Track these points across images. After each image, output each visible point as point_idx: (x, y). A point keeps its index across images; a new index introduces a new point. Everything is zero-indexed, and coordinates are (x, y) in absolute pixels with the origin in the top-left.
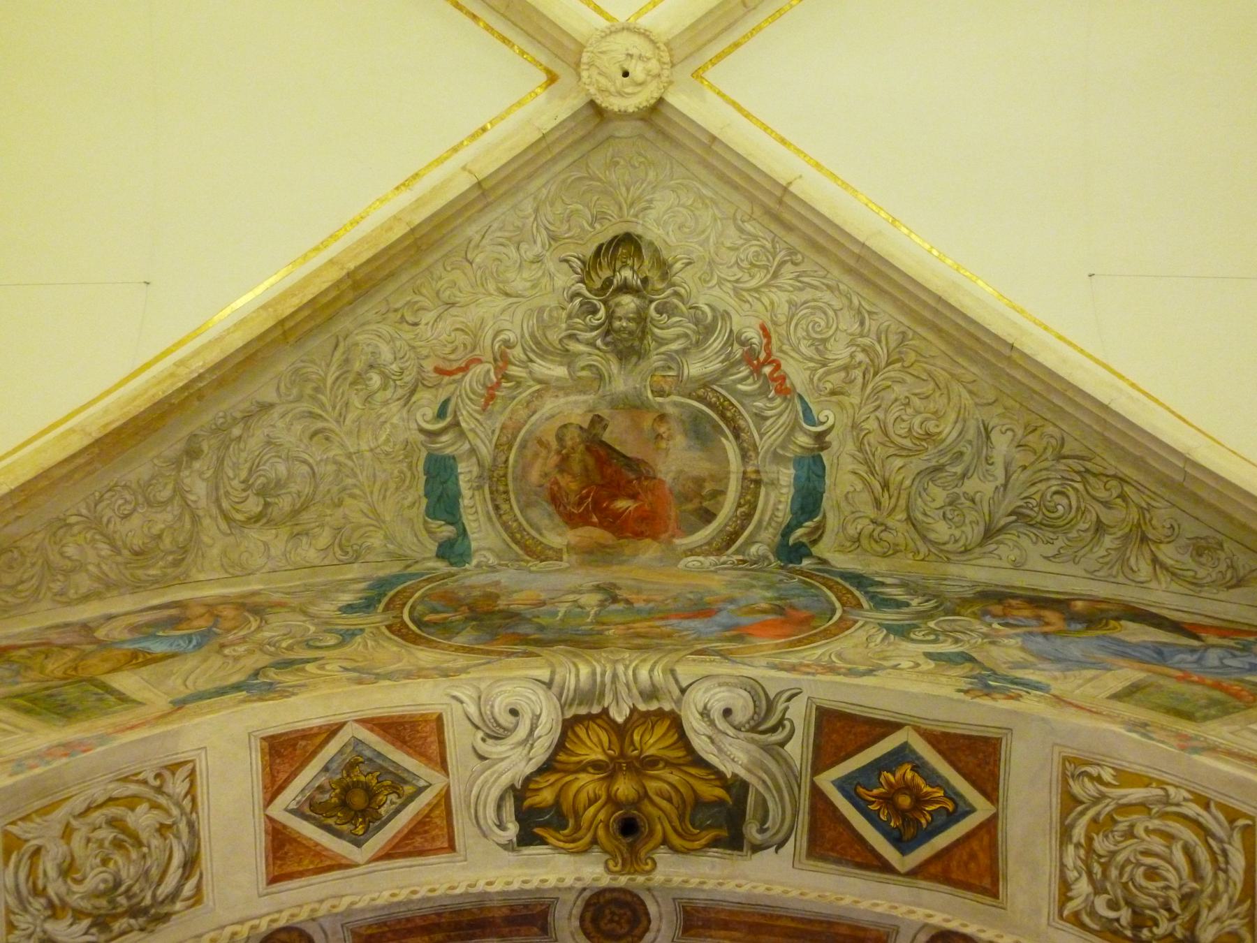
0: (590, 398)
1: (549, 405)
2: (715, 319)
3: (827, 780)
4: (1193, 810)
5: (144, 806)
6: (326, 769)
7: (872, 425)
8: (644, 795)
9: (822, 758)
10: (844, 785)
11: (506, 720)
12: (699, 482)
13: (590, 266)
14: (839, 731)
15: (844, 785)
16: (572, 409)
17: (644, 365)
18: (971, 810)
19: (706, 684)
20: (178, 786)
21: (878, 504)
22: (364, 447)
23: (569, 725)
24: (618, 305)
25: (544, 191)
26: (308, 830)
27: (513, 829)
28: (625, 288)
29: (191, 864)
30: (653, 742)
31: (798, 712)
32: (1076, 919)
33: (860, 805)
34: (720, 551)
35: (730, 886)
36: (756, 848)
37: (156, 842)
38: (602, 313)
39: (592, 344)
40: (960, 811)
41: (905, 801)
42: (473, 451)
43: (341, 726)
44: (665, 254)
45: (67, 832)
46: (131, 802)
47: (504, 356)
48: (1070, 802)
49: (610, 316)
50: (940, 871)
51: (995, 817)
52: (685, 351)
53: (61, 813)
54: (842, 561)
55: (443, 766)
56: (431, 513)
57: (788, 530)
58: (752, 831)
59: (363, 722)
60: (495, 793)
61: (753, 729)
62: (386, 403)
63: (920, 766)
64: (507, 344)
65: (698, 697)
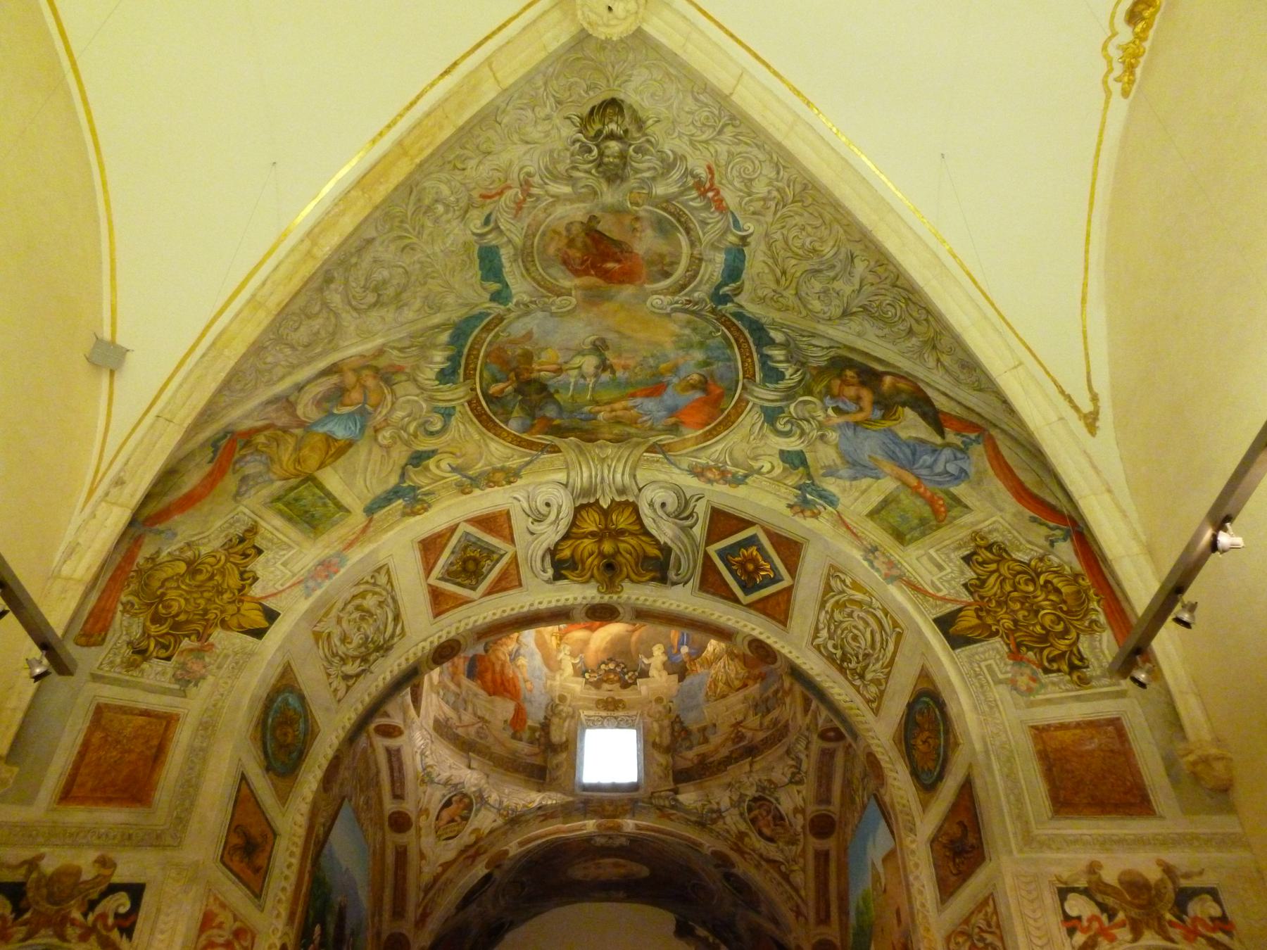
0: (588, 205)
1: (560, 210)
2: (675, 159)
3: (713, 550)
4: (880, 614)
5: (369, 596)
6: (453, 552)
7: (778, 236)
8: (618, 552)
9: (712, 537)
10: (723, 554)
11: (544, 510)
12: (662, 256)
14: (723, 522)
15: (723, 554)
16: (577, 212)
17: (625, 186)
18: (782, 580)
19: (653, 487)
20: (382, 579)
21: (778, 282)
22: (437, 249)
23: (578, 510)
24: (607, 147)
25: (551, 69)
26: (449, 587)
27: (550, 572)
28: (612, 136)
29: (397, 618)
30: (622, 521)
31: (701, 509)
32: (818, 648)
33: (728, 565)
34: (674, 294)
35: (658, 604)
36: (674, 584)
38: (595, 152)
39: (588, 172)
40: (776, 579)
41: (751, 567)
42: (510, 241)
43: (457, 525)
44: (640, 114)
45: (339, 621)
46: (363, 595)
47: (527, 182)
48: (828, 588)
49: (601, 154)
52: (654, 179)
53: (334, 612)
54: (753, 309)
55: (512, 541)
56: (485, 278)
57: (719, 287)
58: (672, 574)
59: (468, 521)
60: (540, 553)
61: (676, 517)
62: (449, 221)
63: (761, 549)
64: (529, 175)
65: (648, 494)
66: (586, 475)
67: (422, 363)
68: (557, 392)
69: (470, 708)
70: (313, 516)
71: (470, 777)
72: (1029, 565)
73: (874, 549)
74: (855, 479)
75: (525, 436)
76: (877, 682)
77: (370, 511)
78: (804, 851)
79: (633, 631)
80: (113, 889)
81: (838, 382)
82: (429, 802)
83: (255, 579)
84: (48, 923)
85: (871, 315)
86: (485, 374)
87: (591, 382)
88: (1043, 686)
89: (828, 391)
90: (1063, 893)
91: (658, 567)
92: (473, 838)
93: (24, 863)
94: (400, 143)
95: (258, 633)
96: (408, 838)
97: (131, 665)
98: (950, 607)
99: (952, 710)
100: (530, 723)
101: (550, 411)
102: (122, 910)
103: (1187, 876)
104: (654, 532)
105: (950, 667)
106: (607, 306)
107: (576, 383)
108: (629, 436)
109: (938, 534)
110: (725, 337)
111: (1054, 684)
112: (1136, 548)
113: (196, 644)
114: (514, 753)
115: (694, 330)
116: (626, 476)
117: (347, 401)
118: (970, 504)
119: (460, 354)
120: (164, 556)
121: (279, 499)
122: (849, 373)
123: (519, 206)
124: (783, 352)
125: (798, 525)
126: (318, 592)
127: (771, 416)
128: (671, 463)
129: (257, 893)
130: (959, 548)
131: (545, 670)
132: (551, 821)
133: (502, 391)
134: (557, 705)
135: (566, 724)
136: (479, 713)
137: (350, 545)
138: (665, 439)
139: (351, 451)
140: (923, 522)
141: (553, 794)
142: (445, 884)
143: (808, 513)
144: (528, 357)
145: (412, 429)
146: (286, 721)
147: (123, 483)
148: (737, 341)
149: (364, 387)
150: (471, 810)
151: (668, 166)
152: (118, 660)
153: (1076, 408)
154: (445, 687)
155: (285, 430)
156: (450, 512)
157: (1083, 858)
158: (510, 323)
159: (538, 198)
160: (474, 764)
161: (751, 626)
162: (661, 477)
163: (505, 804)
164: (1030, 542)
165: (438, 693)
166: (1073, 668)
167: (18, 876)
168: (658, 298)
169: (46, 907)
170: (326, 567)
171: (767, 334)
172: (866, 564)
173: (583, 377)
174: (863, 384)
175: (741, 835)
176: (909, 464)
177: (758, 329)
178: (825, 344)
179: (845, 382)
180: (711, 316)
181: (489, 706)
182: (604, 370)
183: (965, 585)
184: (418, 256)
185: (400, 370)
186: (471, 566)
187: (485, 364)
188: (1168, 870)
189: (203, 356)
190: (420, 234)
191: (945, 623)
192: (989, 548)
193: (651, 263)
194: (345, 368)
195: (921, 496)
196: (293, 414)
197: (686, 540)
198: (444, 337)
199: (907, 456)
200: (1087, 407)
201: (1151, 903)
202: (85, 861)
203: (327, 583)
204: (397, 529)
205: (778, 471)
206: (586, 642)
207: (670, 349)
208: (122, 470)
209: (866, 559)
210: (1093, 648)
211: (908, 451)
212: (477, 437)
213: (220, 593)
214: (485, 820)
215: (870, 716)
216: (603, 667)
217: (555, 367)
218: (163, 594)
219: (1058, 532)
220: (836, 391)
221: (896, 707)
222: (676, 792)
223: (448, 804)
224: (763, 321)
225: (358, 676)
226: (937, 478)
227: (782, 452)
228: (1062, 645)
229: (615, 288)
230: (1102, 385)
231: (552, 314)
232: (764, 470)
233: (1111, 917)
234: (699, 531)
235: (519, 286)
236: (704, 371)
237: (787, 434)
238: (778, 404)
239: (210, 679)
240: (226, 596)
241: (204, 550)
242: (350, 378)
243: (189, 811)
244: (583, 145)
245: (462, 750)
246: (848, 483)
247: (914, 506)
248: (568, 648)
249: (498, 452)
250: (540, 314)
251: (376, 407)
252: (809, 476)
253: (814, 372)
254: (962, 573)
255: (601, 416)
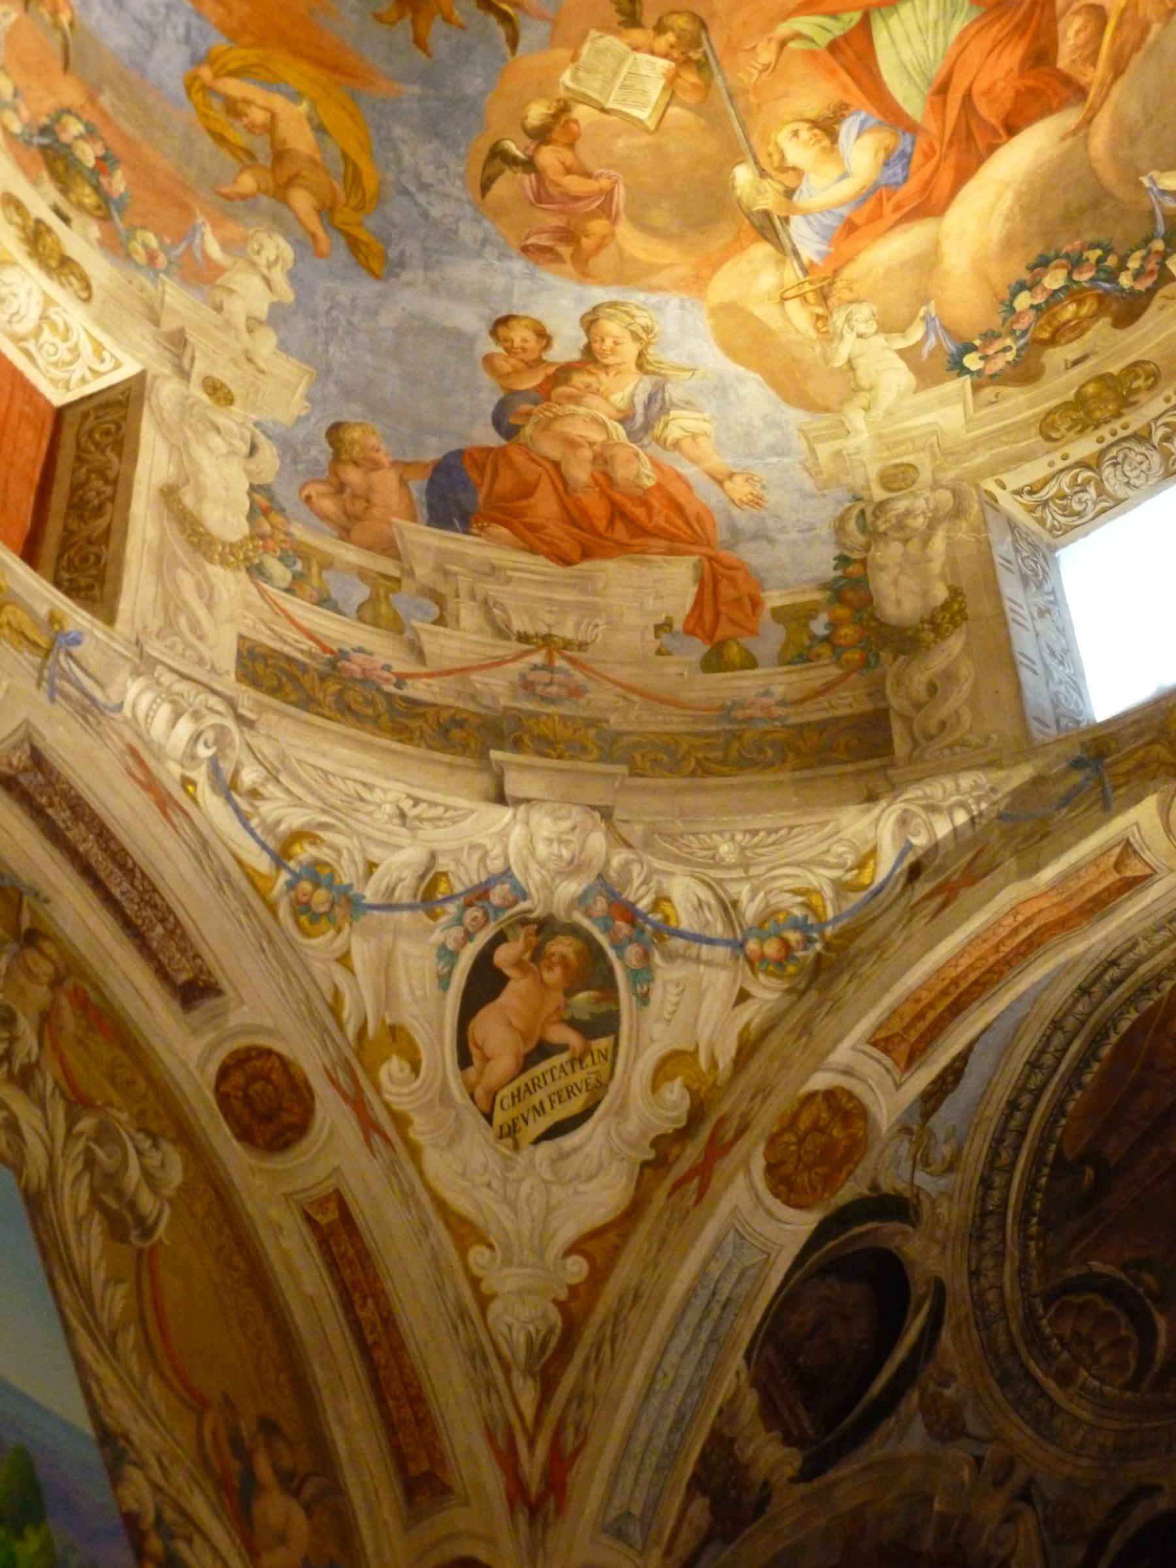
69: (469, 616)
71: (531, 839)
79: (1088, 121)
82: (387, 994)
92: (675, 1094)
96: (333, 1146)
100: (774, 599)
114: (725, 712)
131: (795, 416)
132: (967, 896)
134: (881, 506)
135: (938, 544)
136: (520, 624)
141: (937, 789)
142: (617, 1317)
150: (609, 987)
154: (294, 553)
160: (515, 784)
163: (751, 910)
165: (257, 571)
181: (569, 596)
206: (928, 262)
214: (692, 1009)
216: (1023, 301)
223: (484, 983)
245: (463, 749)
248: (863, 312)
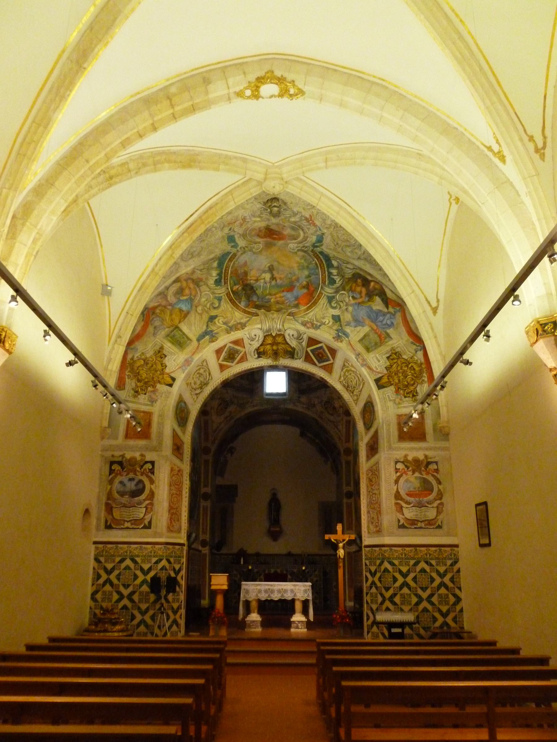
1: (256, 224)
3: (309, 349)
4: (359, 376)
8: (278, 349)
9: (309, 345)
10: (312, 351)
11: (254, 337)
12: (293, 236)
13: (265, 204)
14: (312, 341)
16: (263, 224)
17: (280, 218)
18: (330, 360)
20: (205, 364)
21: (335, 245)
23: (265, 337)
26: (225, 363)
27: (257, 356)
28: (275, 206)
29: (210, 374)
30: (279, 340)
31: (305, 337)
33: (314, 355)
37: (204, 373)
40: (328, 360)
41: (321, 356)
42: (238, 233)
43: (226, 345)
46: (199, 369)
48: (344, 365)
50: (324, 368)
51: (333, 363)
53: (192, 376)
55: (244, 347)
57: (314, 244)
58: (296, 356)
59: (231, 342)
63: (324, 350)
64: (245, 217)
65: (288, 332)
66: (267, 325)
67: (209, 277)
68: (257, 289)
70: (180, 342)
72: (407, 360)
73: (359, 354)
74: (356, 327)
75: (247, 309)
76: (357, 396)
77: (198, 340)
78: (342, 419)
80: (147, 462)
81: (354, 285)
83: (166, 366)
84: (131, 471)
85: (367, 261)
86: (231, 282)
87: (268, 285)
88: (404, 402)
89: (351, 290)
90: (396, 463)
91: (291, 354)
93: (120, 456)
94: (200, 217)
95: (171, 385)
97: (135, 397)
98: (380, 375)
99: (376, 408)
101: (255, 299)
102: (151, 467)
103: (431, 458)
104: (290, 343)
105: (377, 395)
106: (274, 249)
107: (263, 286)
108: (282, 309)
109: (380, 348)
110: (316, 264)
111: (407, 401)
112: (439, 357)
113: (153, 389)
115: (305, 260)
116: (281, 326)
117: (184, 294)
118: (392, 337)
119: (222, 272)
120: (135, 358)
121: (168, 336)
122: (359, 281)
123: (241, 225)
124: (336, 271)
125: (336, 345)
126: (186, 371)
127: (330, 299)
128: (295, 320)
129: (182, 460)
130: (386, 354)
133: (238, 289)
137: (193, 354)
138: (294, 310)
139: (189, 316)
140: (376, 344)
143: (339, 340)
144: (246, 274)
145: (208, 306)
146: (182, 410)
147: (121, 337)
148: (320, 265)
149: (190, 288)
151: (295, 214)
152: (131, 395)
153: (430, 306)
155: (165, 307)
156: (224, 340)
157: (404, 453)
158: (239, 257)
159: (248, 222)
161: (320, 373)
162: (292, 326)
164: (409, 352)
166: (414, 396)
167: (120, 459)
168: (292, 245)
169: (129, 467)
170: (187, 362)
171: (331, 262)
172: (356, 360)
173: (266, 283)
174: (363, 285)
175: (322, 412)
176: (374, 321)
177: (328, 259)
178: (351, 267)
179: (357, 285)
180: (311, 254)
182: (273, 280)
183: (386, 368)
184: (206, 242)
185: (201, 280)
186: (232, 356)
187: (231, 277)
188: (426, 456)
189: (139, 291)
190: (207, 236)
191: (377, 381)
192: (395, 354)
193: (289, 236)
194: (182, 280)
195: (376, 333)
196: (167, 300)
197: (300, 346)
198: (215, 264)
199: (374, 317)
200: (434, 304)
201: (419, 465)
202: (137, 455)
203: (189, 368)
204: (208, 347)
205: (331, 323)
207: (296, 268)
208: (119, 332)
209: (356, 358)
210: (421, 389)
211: (375, 315)
212: (230, 309)
213: (156, 371)
215: (354, 405)
217: (254, 278)
218: (139, 372)
219: (419, 348)
220: (353, 288)
221: (361, 404)
222: (299, 397)
224: (330, 255)
225: (200, 393)
226: (384, 326)
227: (333, 315)
228: (412, 388)
229: (276, 241)
230: (441, 297)
231: (254, 253)
232: (326, 323)
233: (408, 469)
234: (304, 344)
235: (241, 243)
236: (307, 280)
237: (334, 308)
238: (333, 295)
239: (159, 401)
240: (158, 372)
241: (148, 356)
242: (184, 284)
243: (162, 440)
244: (264, 209)
246: (353, 329)
247: (374, 337)
249: (238, 316)
250: (249, 253)
251: (195, 296)
252: (341, 326)
253: (347, 280)
254: (386, 363)
255: (272, 300)
